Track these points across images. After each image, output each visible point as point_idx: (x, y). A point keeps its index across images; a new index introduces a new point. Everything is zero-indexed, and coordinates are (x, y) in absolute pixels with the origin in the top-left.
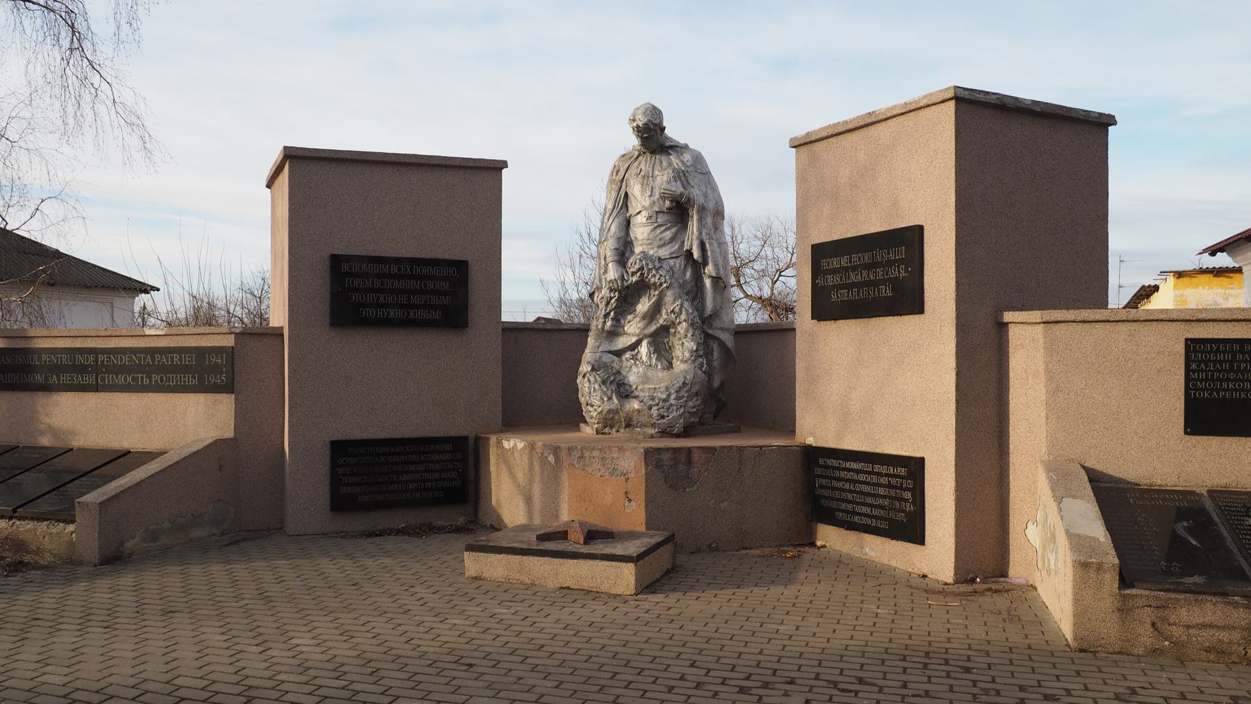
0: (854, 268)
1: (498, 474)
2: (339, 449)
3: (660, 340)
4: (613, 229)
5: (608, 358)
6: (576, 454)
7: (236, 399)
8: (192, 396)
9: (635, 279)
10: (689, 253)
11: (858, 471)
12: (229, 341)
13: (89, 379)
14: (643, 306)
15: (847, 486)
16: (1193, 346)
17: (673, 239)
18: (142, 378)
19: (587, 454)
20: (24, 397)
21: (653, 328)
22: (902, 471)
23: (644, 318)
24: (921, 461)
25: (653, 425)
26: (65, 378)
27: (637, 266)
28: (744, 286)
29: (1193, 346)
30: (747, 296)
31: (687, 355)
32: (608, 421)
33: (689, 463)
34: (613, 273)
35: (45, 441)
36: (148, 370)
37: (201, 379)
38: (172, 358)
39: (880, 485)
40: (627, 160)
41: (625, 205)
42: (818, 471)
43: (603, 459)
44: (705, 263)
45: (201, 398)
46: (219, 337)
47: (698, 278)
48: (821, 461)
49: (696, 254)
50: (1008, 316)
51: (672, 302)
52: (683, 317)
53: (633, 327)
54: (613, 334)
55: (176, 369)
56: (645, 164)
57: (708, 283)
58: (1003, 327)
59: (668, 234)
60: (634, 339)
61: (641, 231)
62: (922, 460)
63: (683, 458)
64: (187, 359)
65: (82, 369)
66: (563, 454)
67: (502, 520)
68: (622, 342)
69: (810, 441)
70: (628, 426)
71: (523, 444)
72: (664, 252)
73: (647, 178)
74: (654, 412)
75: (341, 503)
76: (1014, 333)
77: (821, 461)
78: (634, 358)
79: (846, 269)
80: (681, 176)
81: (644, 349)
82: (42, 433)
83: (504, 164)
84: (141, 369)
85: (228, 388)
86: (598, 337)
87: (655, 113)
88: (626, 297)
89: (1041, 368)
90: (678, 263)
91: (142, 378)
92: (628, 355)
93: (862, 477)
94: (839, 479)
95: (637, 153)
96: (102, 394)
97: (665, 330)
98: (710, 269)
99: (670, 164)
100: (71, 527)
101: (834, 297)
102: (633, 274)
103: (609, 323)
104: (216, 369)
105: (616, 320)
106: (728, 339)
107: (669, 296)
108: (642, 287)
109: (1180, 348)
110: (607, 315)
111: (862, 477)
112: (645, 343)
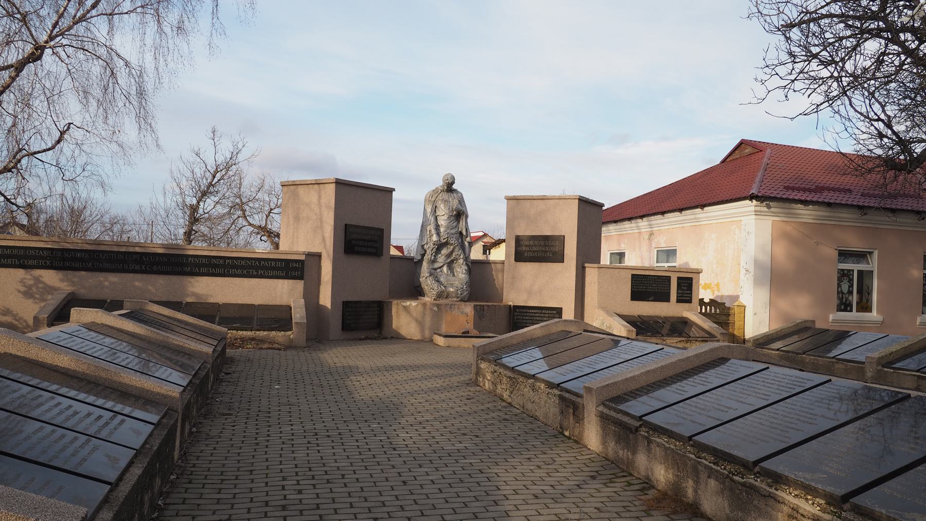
0: (535, 246)
1: (398, 316)
2: (346, 304)
3: (450, 265)
4: (432, 220)
5: (433, 271)
6: (449, 307)
7: (305, 284)
8: (280, 281)
9: (444, 241)
10: (461, 233)
11: (535, 313)
12: (303, 258)
13: (218, 271)
14: (445, 251)
15: (530, 318)
16: (633, 276)
17: (456, 227)
18: (253, 272)
19: (453, 307)
20: (174, 279)
21: (449, 260)
22: (555, 312)
23: (446, 256)
24: (561, 309)
25: (458, 298)
26: (203, 270)
27: (446, 236)
28: (248, 217)
29: (633, 276)
30: (250, 224)
31: (464, 271)
32: (440, 296)
33: (483, 310)
34: (435, 238)
35: (189, 300)
36: (257, 268)
37: (287, 274)
38: (271, 264)
39: (544, 317)
40: (436, 193)
41: (435, 211)
42: (516, 314)
43: (459, 308)
44: (467, 237)
45: (286, 281)
46: (296, 255)
47: (463, 242)
48: (517, 310)
49: (464, 234)
50: (586, 265)
51: (458, 252)
52: (462, 257)
53: (441, 259)
54: (434, 261)
55: (273, 268)
56: (445, 196)
57: (466, 244)
58: (584, 268)
59: (455, 224)
60: (442, 264)
61: (442, 221)
62: (561, 309)
63: (482, 308)
64: (279, 264)
65: (216, 266)
66: (442, 307)
67: (400, 334)
68: (436, 265)
69: (510, 303)
70: (446, 297)
71: (416, 304)
72: (453, 231)
73: (446, 202)
74: (459, 292)
75: (345, 327)
76: (587, 270)
77: (517, 310)
78: (441, 271)
79: (532, 246)
80: (460, 202)
81: (445, 269)
82: (188, 295)
83: (394, 190)
84: (251, 267)
85: (301, 278)
86: (428, 263)
87: (453, 178)
88: (440, 246)
89: (597, 281)
90: (458, 234)
91: (253, 272)
92: (439, 270)
93: (537, 315)
94: (526, 316)
95: (440, 191)
96: (226, 279)
97: (452, 261)
98: (468, 239)
99: (455, 197)
100: (289, 333)
101: (526, 254)
102: (444, 239)
103: (433, 258)
104: (296, 269)
105: (434, 256)
106: (470, 264)
107: (457, 249)
108: (446, 244)
109: (630, 277)
110: (432, 254)
111: (537, 315)
112: (445, 266)
